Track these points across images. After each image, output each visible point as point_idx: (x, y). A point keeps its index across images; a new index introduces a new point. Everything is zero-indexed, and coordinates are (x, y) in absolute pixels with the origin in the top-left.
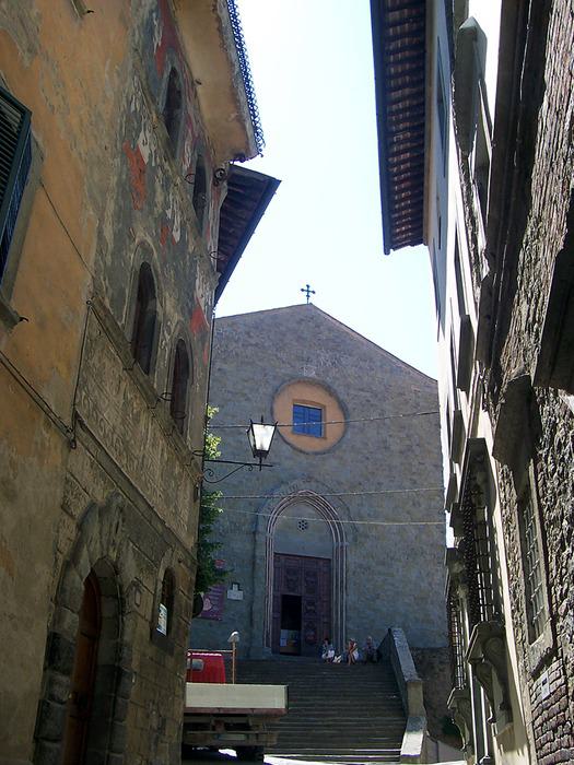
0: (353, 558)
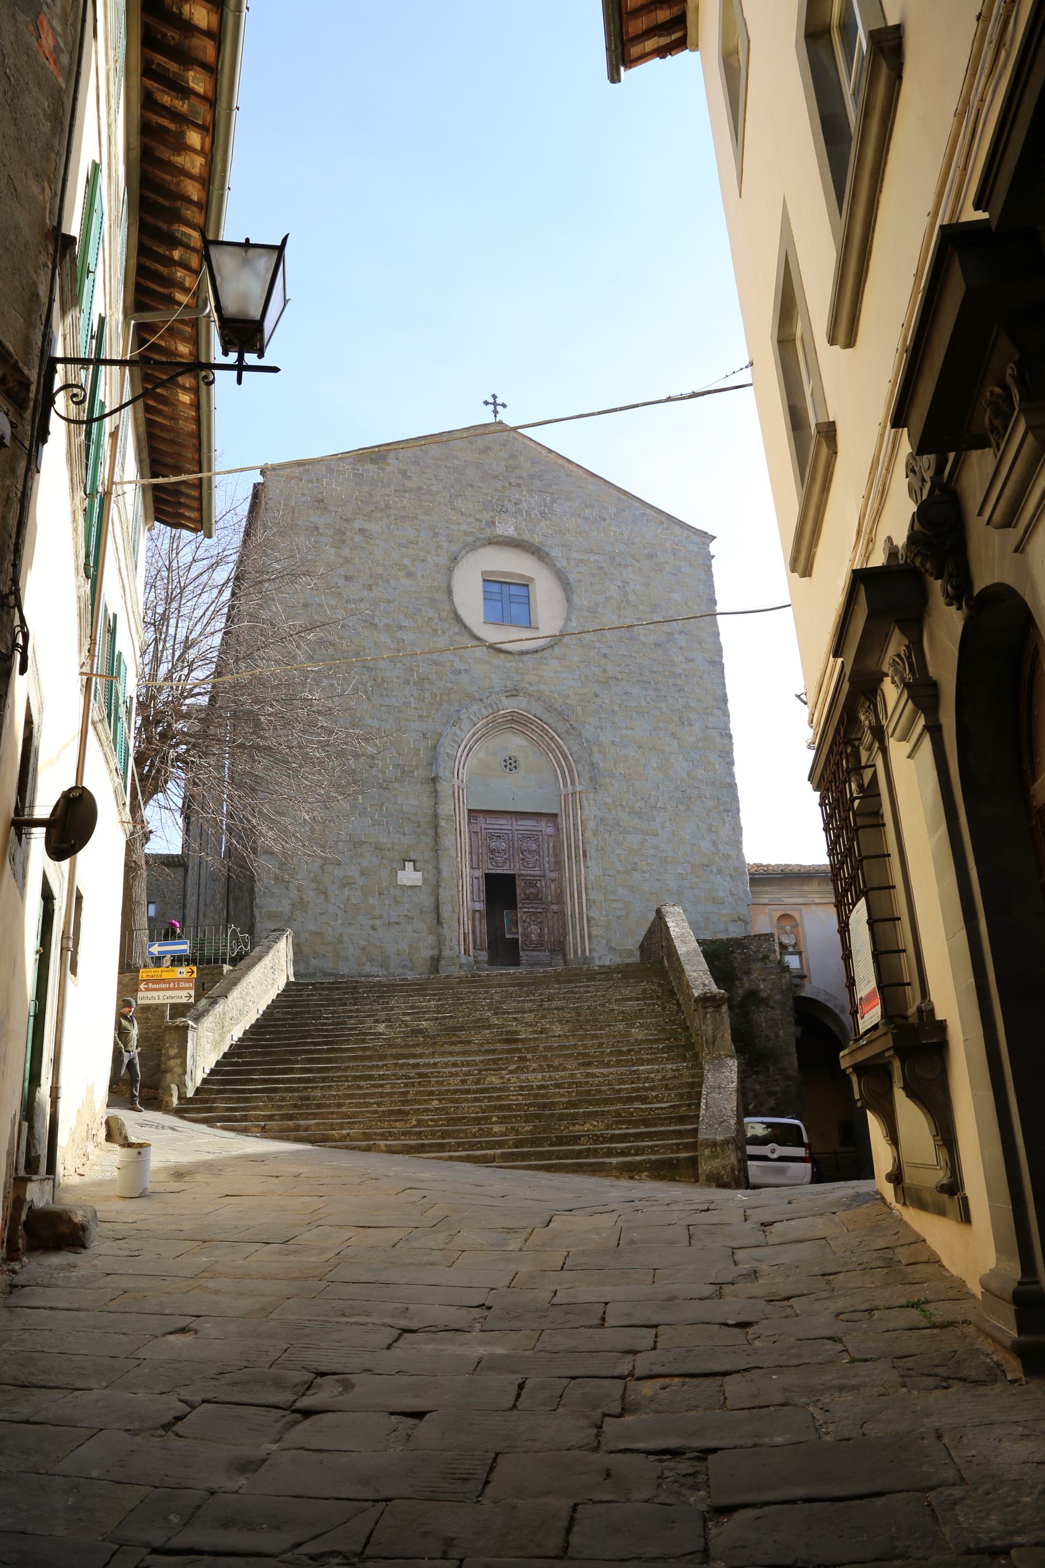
0: (591, 810)
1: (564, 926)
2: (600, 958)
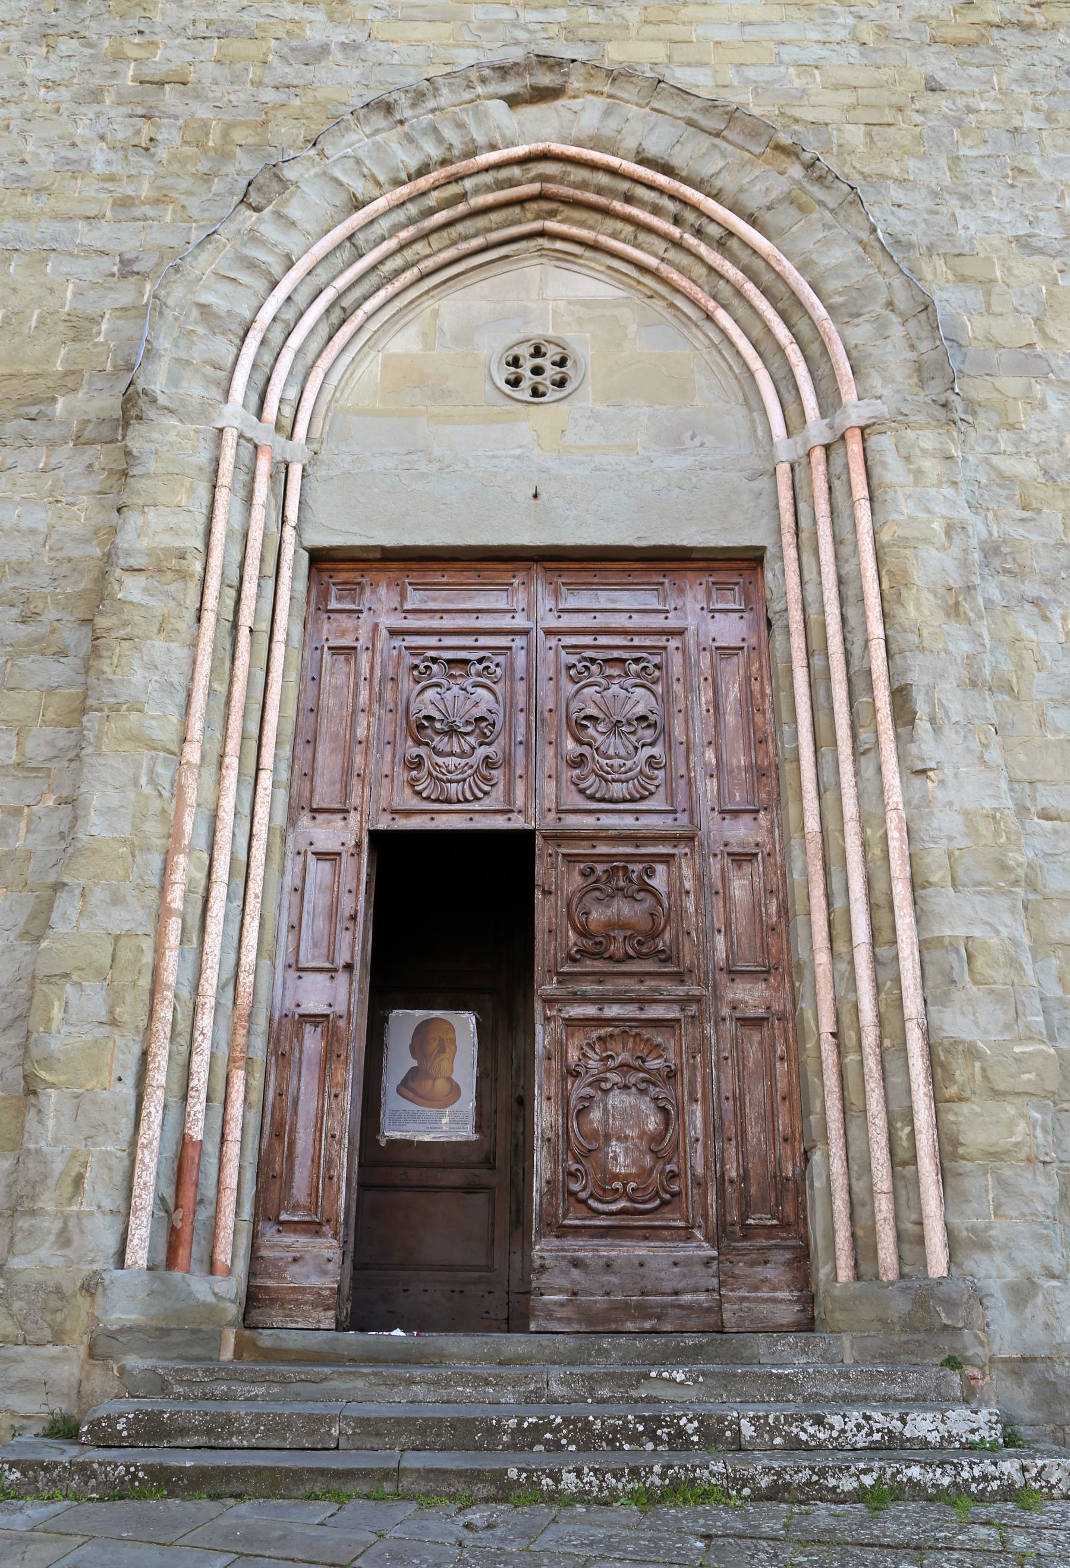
1: (799, 1097)
2: (1021, 1294)
